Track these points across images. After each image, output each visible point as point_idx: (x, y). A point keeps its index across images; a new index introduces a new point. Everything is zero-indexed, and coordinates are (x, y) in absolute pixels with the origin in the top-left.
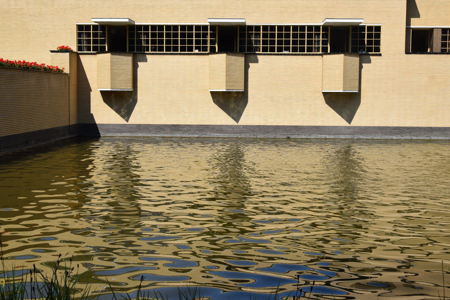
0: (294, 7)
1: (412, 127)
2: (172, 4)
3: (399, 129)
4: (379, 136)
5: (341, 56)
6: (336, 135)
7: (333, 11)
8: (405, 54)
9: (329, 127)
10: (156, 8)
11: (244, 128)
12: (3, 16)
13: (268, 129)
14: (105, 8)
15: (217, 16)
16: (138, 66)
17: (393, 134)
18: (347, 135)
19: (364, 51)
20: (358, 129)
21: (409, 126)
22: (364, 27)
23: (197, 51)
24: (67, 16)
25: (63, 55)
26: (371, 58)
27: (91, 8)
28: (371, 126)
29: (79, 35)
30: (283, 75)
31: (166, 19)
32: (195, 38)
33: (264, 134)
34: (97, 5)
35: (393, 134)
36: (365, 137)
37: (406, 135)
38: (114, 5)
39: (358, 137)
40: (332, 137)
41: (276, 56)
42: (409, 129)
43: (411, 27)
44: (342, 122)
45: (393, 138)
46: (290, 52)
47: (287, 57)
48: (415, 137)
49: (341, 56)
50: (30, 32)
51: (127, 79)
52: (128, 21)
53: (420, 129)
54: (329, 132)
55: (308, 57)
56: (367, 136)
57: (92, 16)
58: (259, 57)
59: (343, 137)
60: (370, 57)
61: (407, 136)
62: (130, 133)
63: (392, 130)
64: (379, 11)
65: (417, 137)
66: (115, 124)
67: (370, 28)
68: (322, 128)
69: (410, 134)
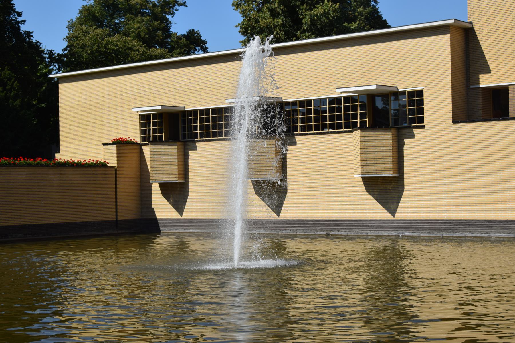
0: (329, 75)
1: (465, 221)
3: (450, 222)
6: (379, 230)
7: (369, 76)
8: (452, 124)
10: (202, 91)
11: (285, 223)
16: (188, 155)
17: (444, 229)
18: (391, 230)
19: (406, 123)
20: (402, 224)
21: (463, 219)
25: (112, 147)
26: (414, 131)
29: (142, 125)
30: (321, 158)
33: (304, 230)
35: (444, 229)
36: (411, 233)
37: (460, 231)
40: (374, 233)
42: (462, 222)
43: (481, 86)
44: (387, 216)
45: (444, 235)
48: (470, 234)
51: (171, 169)
52: (160, 108)
53: (475, 222)
54: (370, 227)
55: (344, 135)
56: (413, 232)
59: (385, 233)
61: (461, 232)
62: (183, 228)
63: (442, 224)
64: (420, 71)
65: (473, 233)
66: (171, 219)
68: (363, 222)
69: (464, 229)
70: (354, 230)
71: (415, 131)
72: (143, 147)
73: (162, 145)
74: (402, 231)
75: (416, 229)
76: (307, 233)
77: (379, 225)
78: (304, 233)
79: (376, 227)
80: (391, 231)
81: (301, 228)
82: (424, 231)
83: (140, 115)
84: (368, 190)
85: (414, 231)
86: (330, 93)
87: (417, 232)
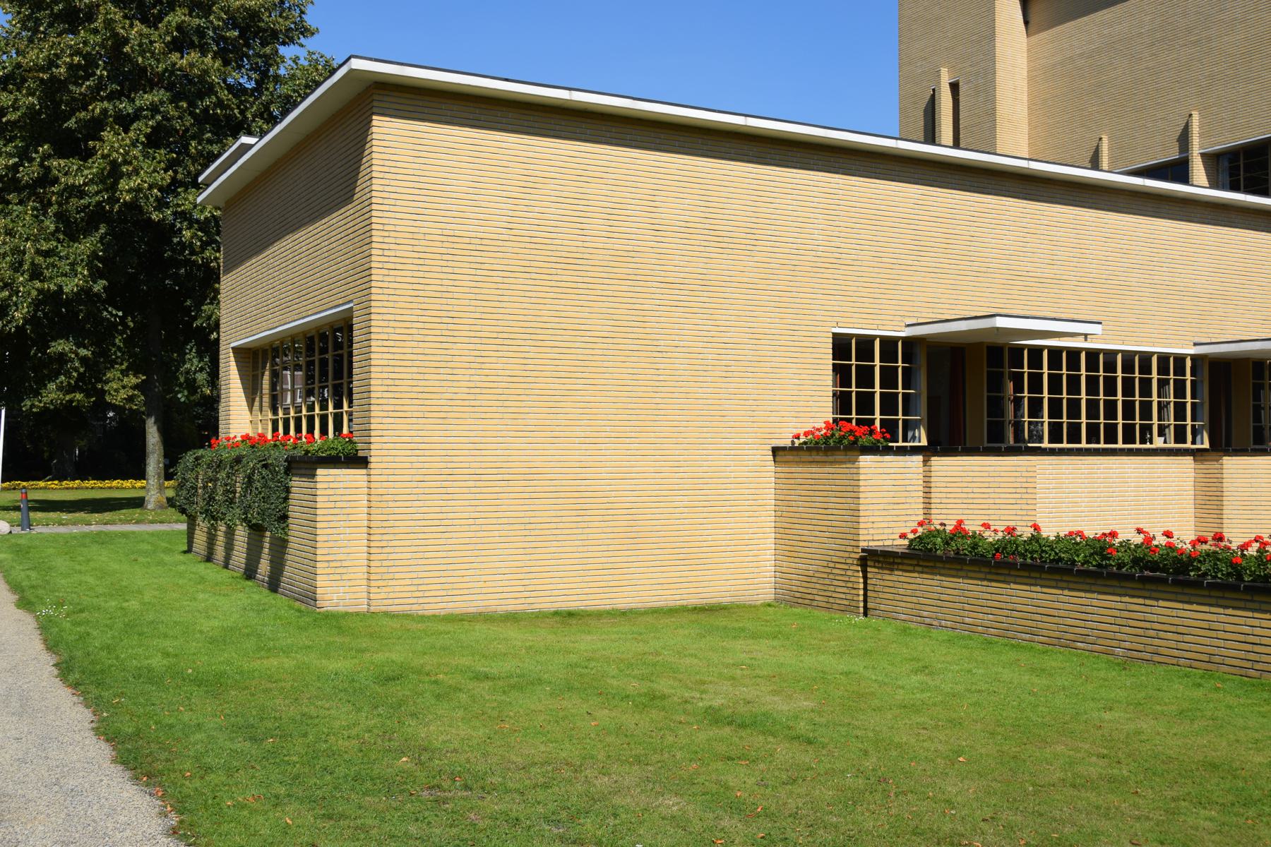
2: (1104, 277)
12: (559, 278)
34: (900, 262)
50: (664, 355)
83: (833, 334)
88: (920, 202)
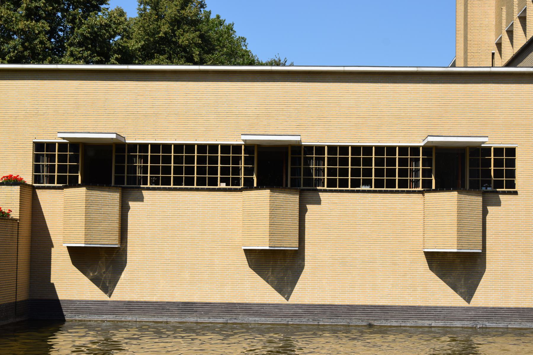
2: (185, 111)
4: (517, 323)
5: (453, 195)
6: (448, 320)
9: (435, 308)
13: (337, 310)
14: (79, 116)
15: (256, 130)
16: (128, 208)
18: (466, 321)
19: (490, 187)
20: (482, 312)
22: (489, 149)
23: (223, 185)
24: (19, 128)
25: (10, 189)
27: (57, 116)
28: (504, 306)
29: (37, 158)
31: (175, 134)
32: (221, 164)
33: (330, 318)
34: (67, 112)
36: (494, 324)
38: (93, 112)
39: (483, 325)
40: (440, 324)
41: (350, 194)
44: (457, 301)
46: (371, 187)
47: (368, 196)
49: (453, 195)
52: (115, 137)
54: (435, 316)
55: (400, 196)
56: (497, 322)
57: (59, 128)
58: (145, 193)
59: (458, 324)
60: (500, 196)
62: (113, 315)
64: (512, 124)
67: (498, 151)
70: (410, 320)
71: (501, 197)
72: (38, 192)
73: (109, 191)
74: (482, 321)
75: (502, 319)
76: (336, 324)
77: (448, 314)
78: (331, 323)
79: (444, 316)
80: (465, 322)
81: (327, 316)
82: (512, 321)
83: (33, 142)
84: (431, 268)
85: (499, 322)
86: (380, 140)
87: (503, 322)
88: (79, 87)
